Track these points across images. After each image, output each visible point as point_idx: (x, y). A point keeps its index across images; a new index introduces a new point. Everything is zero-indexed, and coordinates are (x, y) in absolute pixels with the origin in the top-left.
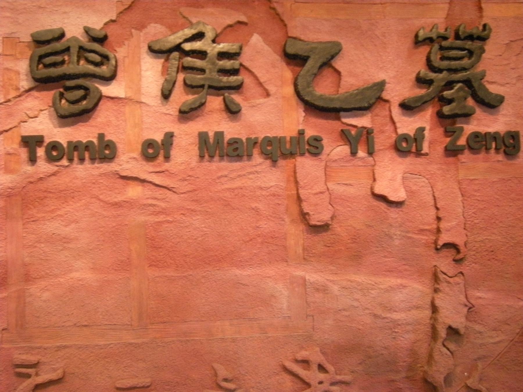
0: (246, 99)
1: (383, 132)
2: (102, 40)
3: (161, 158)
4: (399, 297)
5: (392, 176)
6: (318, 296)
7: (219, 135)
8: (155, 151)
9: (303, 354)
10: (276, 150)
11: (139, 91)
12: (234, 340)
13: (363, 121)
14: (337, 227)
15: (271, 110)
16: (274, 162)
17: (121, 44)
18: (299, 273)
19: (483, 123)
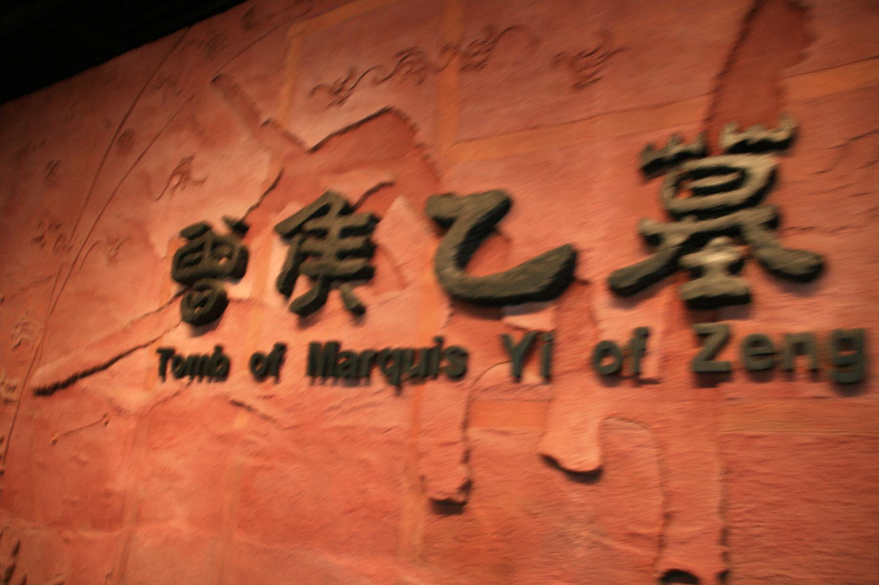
1: (575, 339)
5: (579, 421)
7: (335, 346)
8: (267, 366)
10: (408, 368)
13: (537, 321)
14: (477, 507)
15: (404, 309)
19: (785, 317)
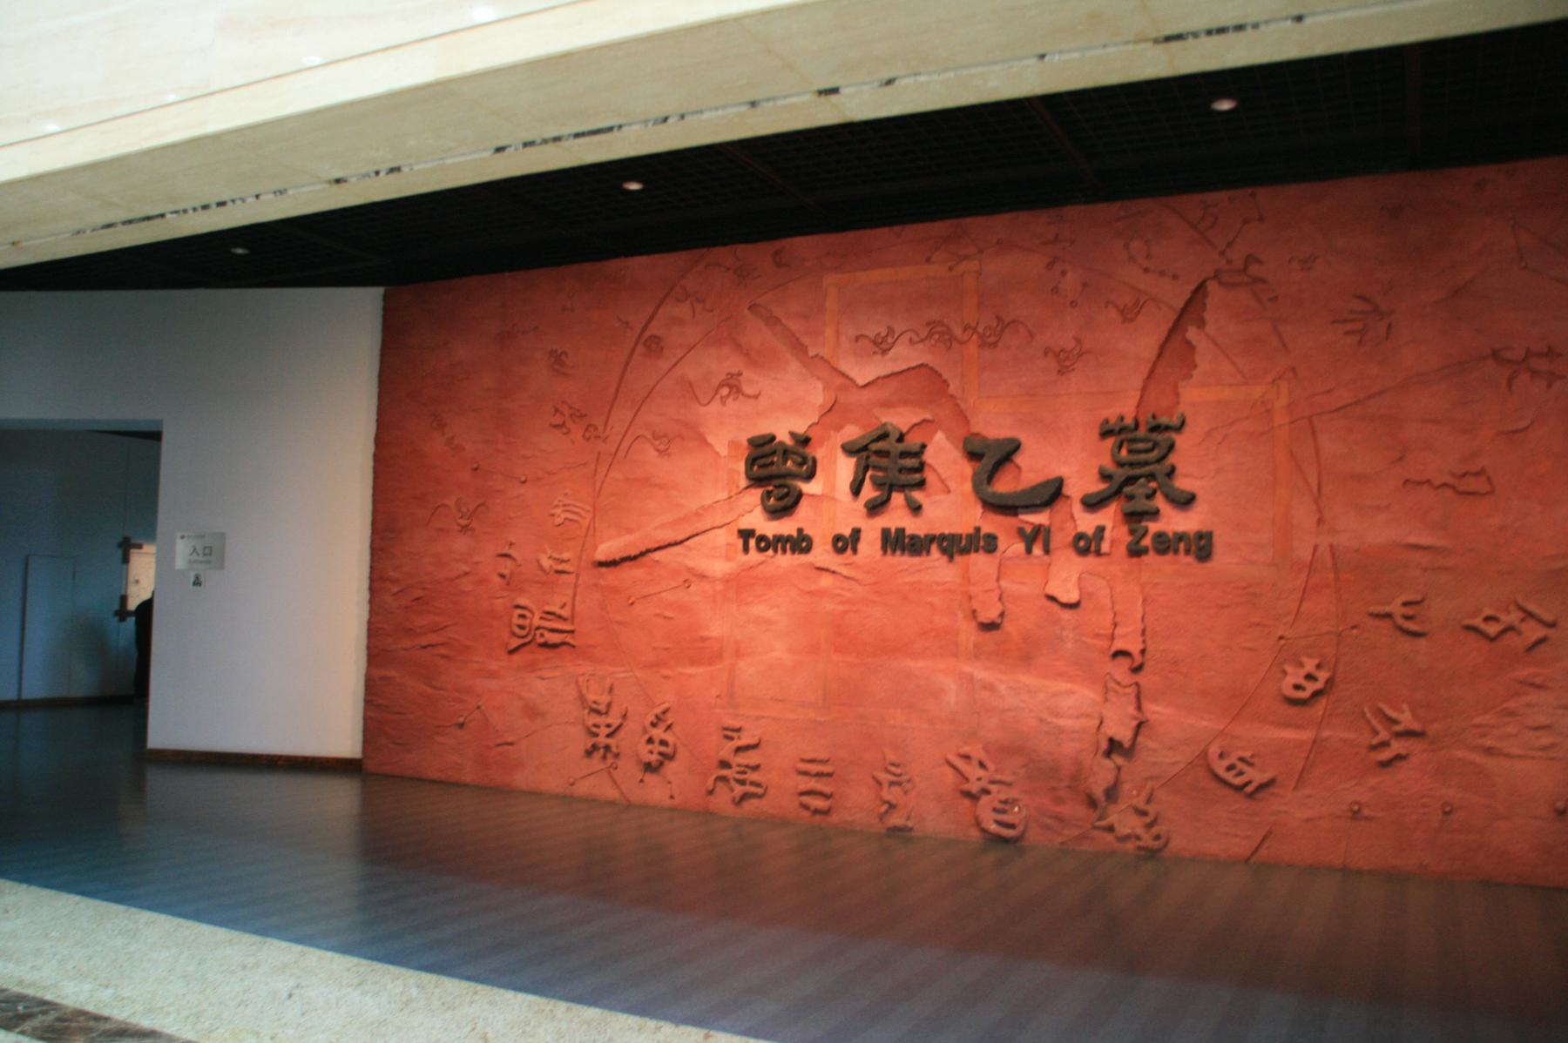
0: (928, 496)
1: (1062, 529)
2: (805, 441)
3: (849, 551)
4: (1066, 703)
5: (1067, 576)
6: (985, 694)
7: (901, 531)
8: (846, 543)
9: (966, 749)
10: (953, 546)
11: (833, 488)
12: (903, 728)
13: (1040, 518)
14: (1007, 625)
15: (949, 505)
16: (951, 558)
17: (821, 444)
18: (968, 669)
19: (1174, 522)
